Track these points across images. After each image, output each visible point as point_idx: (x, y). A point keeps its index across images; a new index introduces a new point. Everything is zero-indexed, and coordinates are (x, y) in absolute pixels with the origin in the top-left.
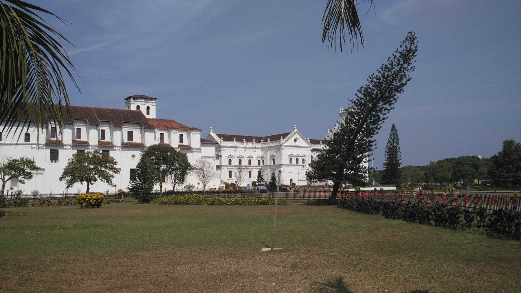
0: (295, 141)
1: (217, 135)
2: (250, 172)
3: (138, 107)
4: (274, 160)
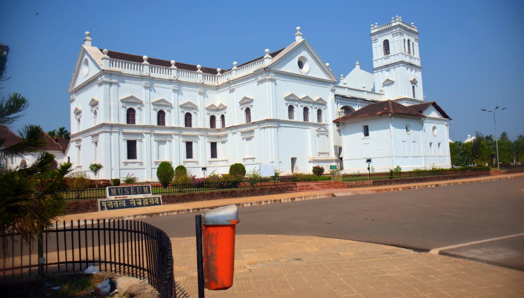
0: (301, 64)
2: (189, 145)
4: (248, 111)
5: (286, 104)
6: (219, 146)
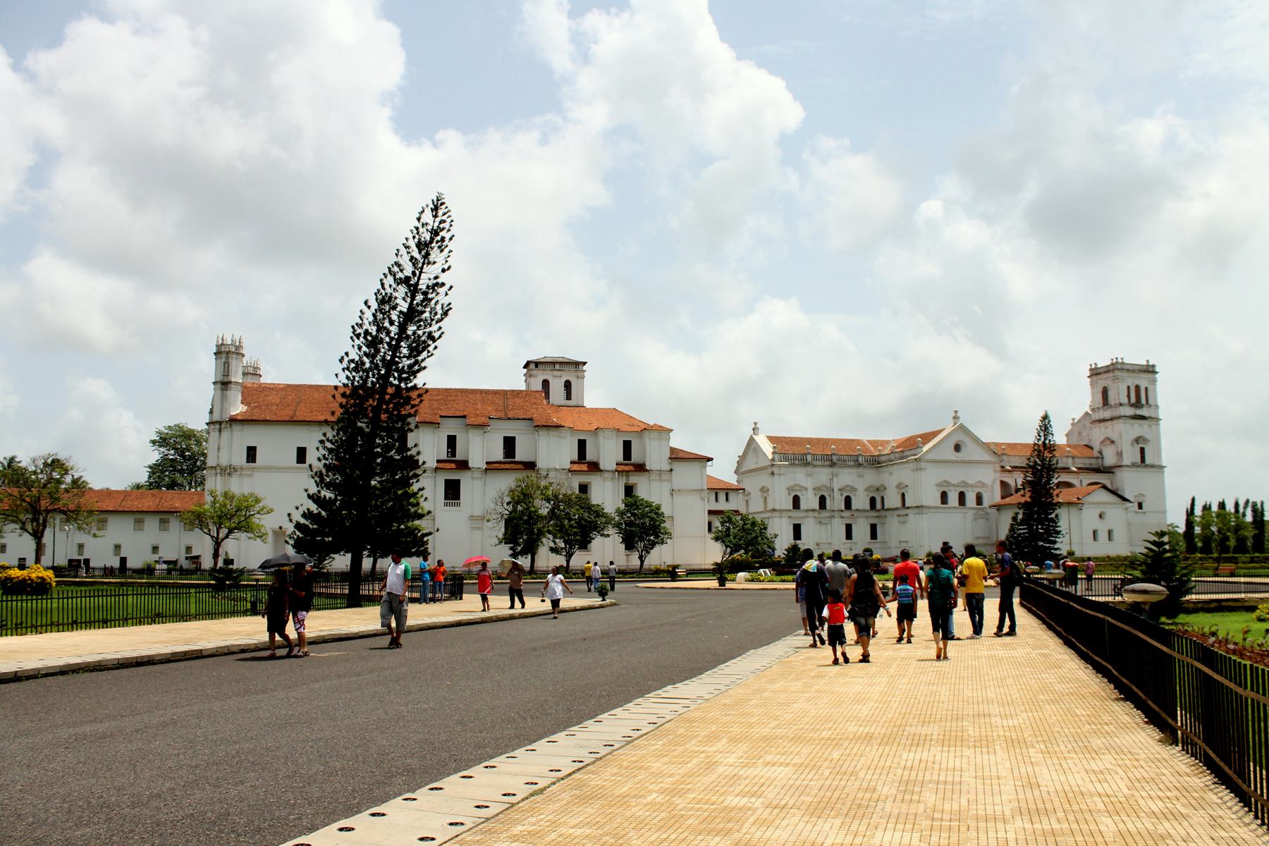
0: (957, 448)
1: (771, 439)
2: (849, 528)
3: (546, 383)
4: (903, 495)
5: (938, 491)
6: (879, 528)
